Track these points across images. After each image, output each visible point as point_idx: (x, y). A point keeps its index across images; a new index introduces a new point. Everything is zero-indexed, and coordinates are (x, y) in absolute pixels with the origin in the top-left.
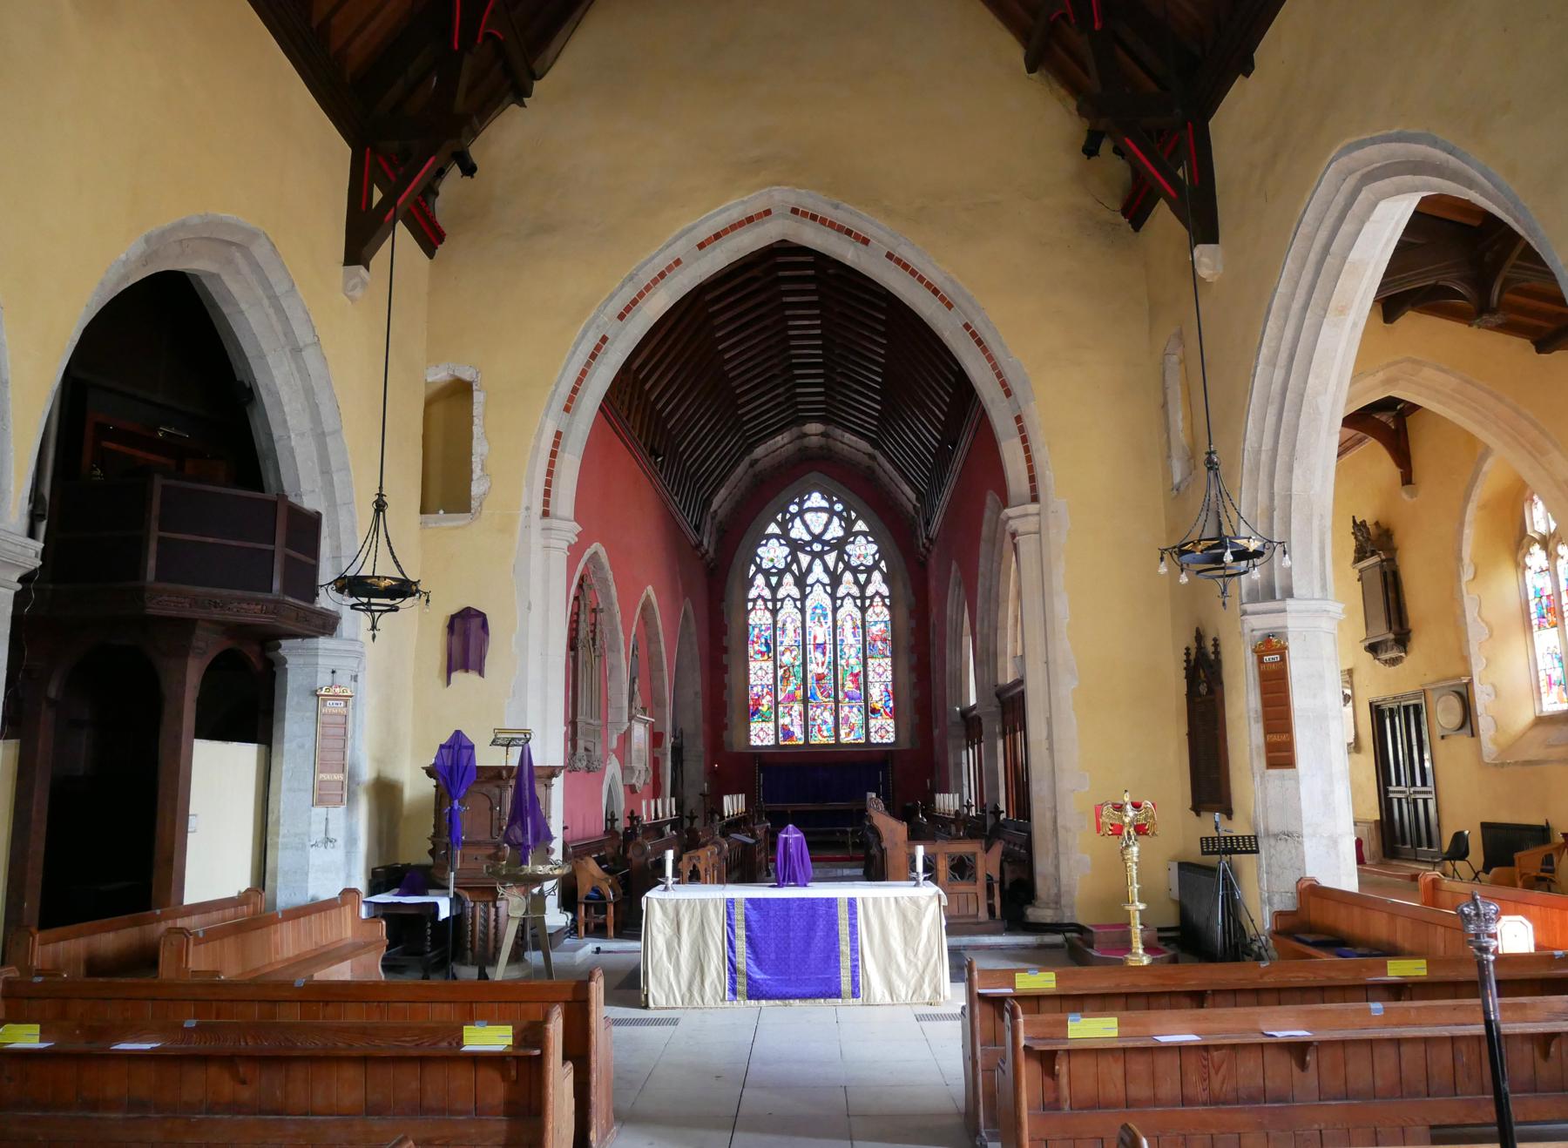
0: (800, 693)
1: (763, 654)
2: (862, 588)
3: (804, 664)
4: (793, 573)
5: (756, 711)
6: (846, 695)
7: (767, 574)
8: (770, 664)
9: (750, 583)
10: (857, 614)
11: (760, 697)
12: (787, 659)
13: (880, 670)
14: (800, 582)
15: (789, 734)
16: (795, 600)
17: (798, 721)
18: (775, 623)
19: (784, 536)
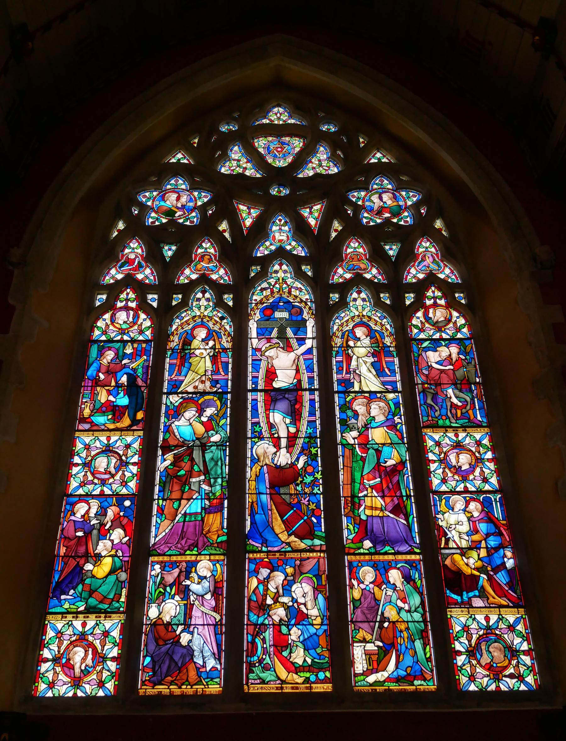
0: (217, 523)
1: (116, 412)
2: (395, 268)
3: (237, 443)
4: (218, 238)
5: (76, 576)
6: (365, 530)
7: (154, 238)
8: (134, 440)
9: (111, 253)
10: (385, 324)
11: (95, 531)
12: (186, 427)
13: (464, 460)
14: (240, 254)
15: (174, 660)
16: (219, 289)
17: (205, 613)
18: (161, 336)
19: (202, 174)
